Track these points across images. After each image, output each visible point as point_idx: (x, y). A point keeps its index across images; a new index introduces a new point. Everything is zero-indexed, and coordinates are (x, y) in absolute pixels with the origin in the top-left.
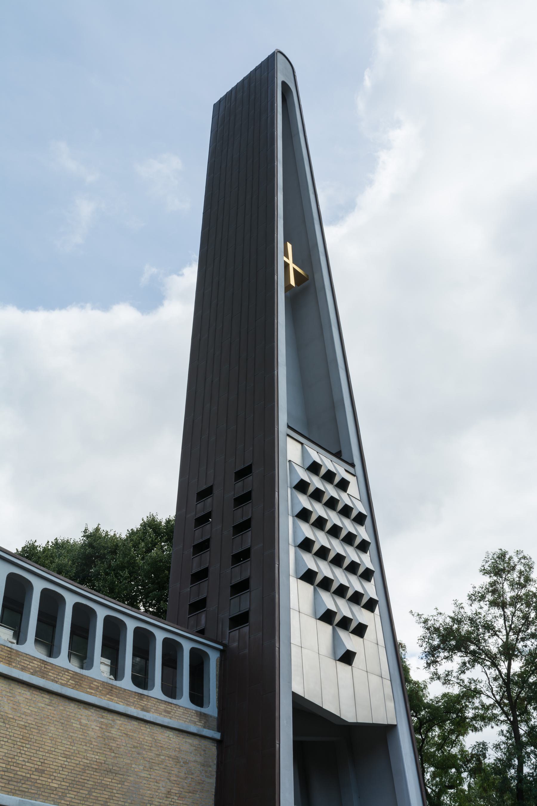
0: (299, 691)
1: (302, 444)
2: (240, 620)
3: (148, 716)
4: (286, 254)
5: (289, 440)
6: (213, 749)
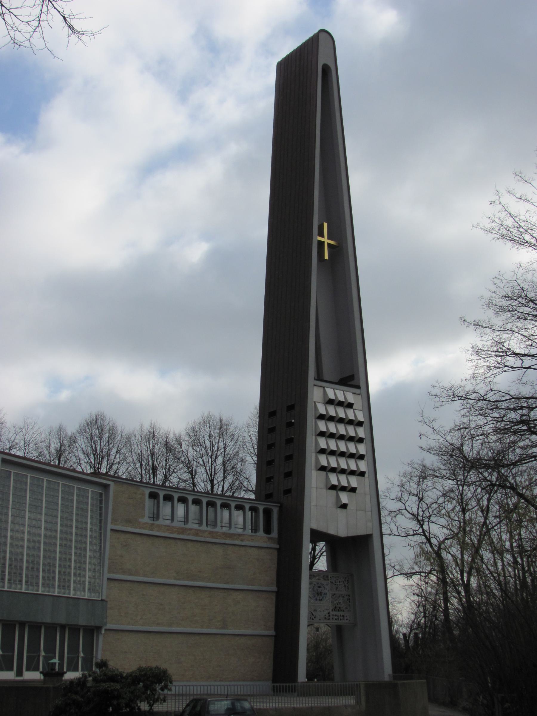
0: (314, 527)
1: (324, 387)
2: (288, 492)
3: (243, 543)
4: (321, 234)
5: (315, 388)
6: (276, 553)
